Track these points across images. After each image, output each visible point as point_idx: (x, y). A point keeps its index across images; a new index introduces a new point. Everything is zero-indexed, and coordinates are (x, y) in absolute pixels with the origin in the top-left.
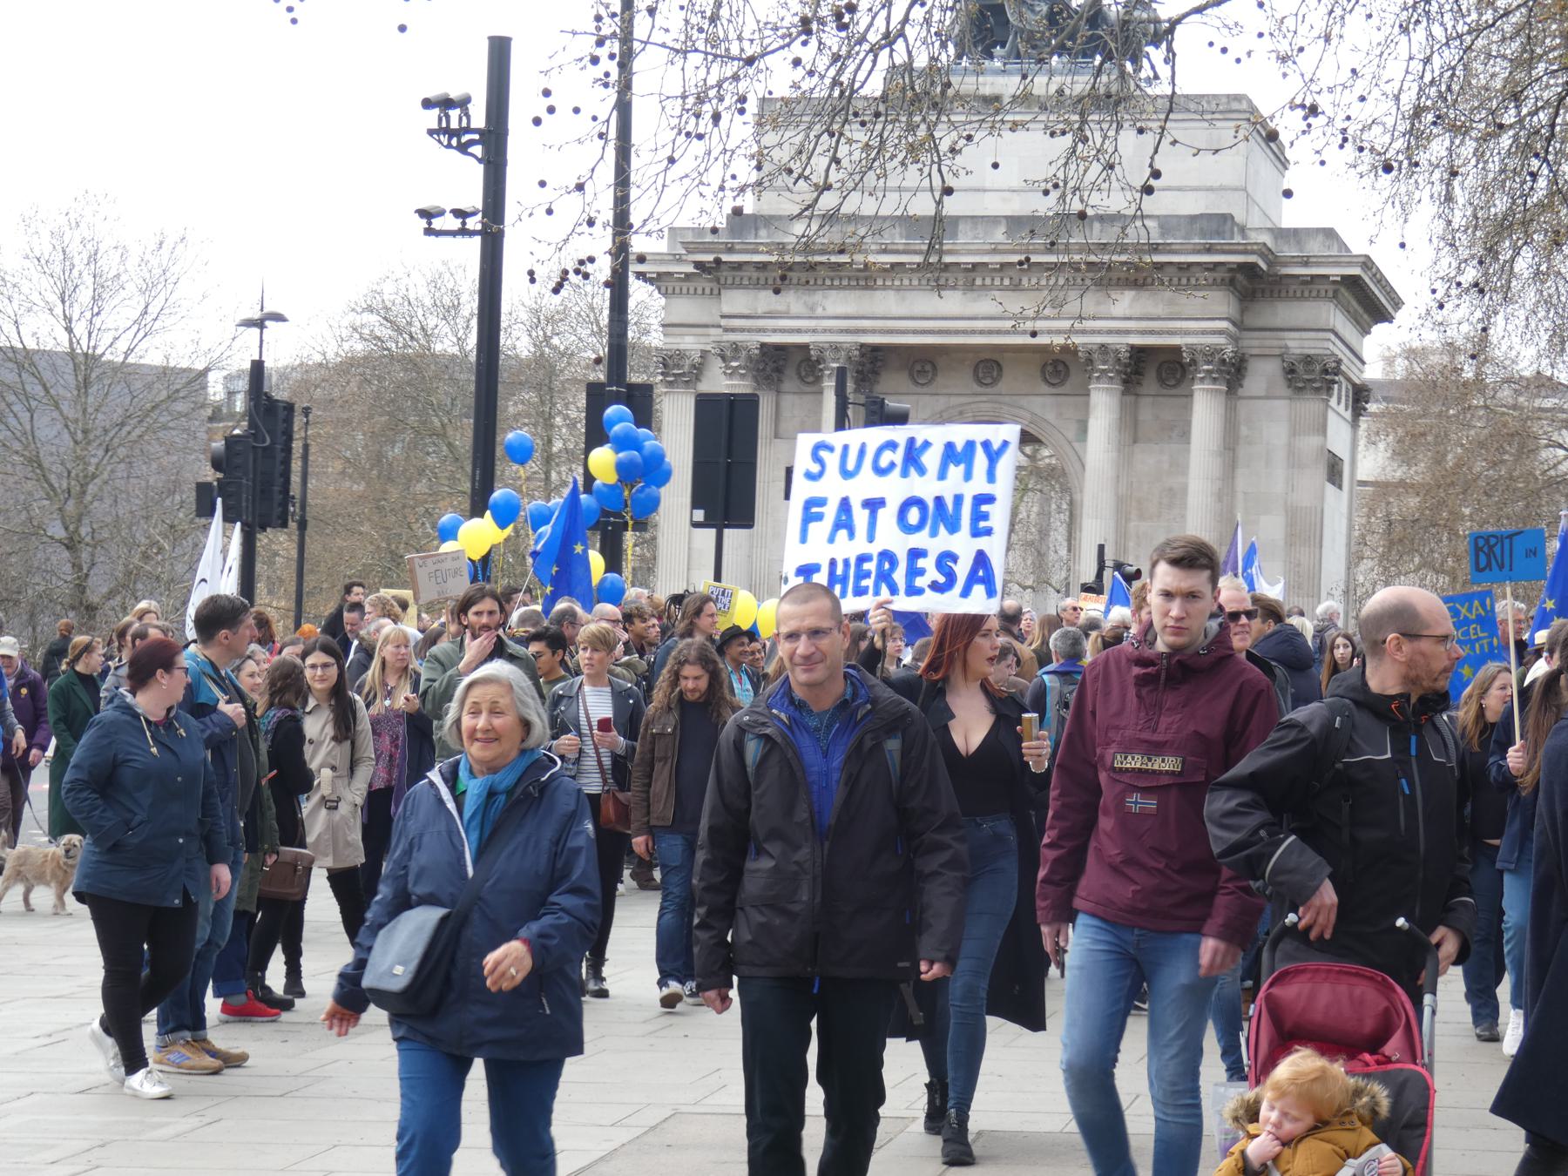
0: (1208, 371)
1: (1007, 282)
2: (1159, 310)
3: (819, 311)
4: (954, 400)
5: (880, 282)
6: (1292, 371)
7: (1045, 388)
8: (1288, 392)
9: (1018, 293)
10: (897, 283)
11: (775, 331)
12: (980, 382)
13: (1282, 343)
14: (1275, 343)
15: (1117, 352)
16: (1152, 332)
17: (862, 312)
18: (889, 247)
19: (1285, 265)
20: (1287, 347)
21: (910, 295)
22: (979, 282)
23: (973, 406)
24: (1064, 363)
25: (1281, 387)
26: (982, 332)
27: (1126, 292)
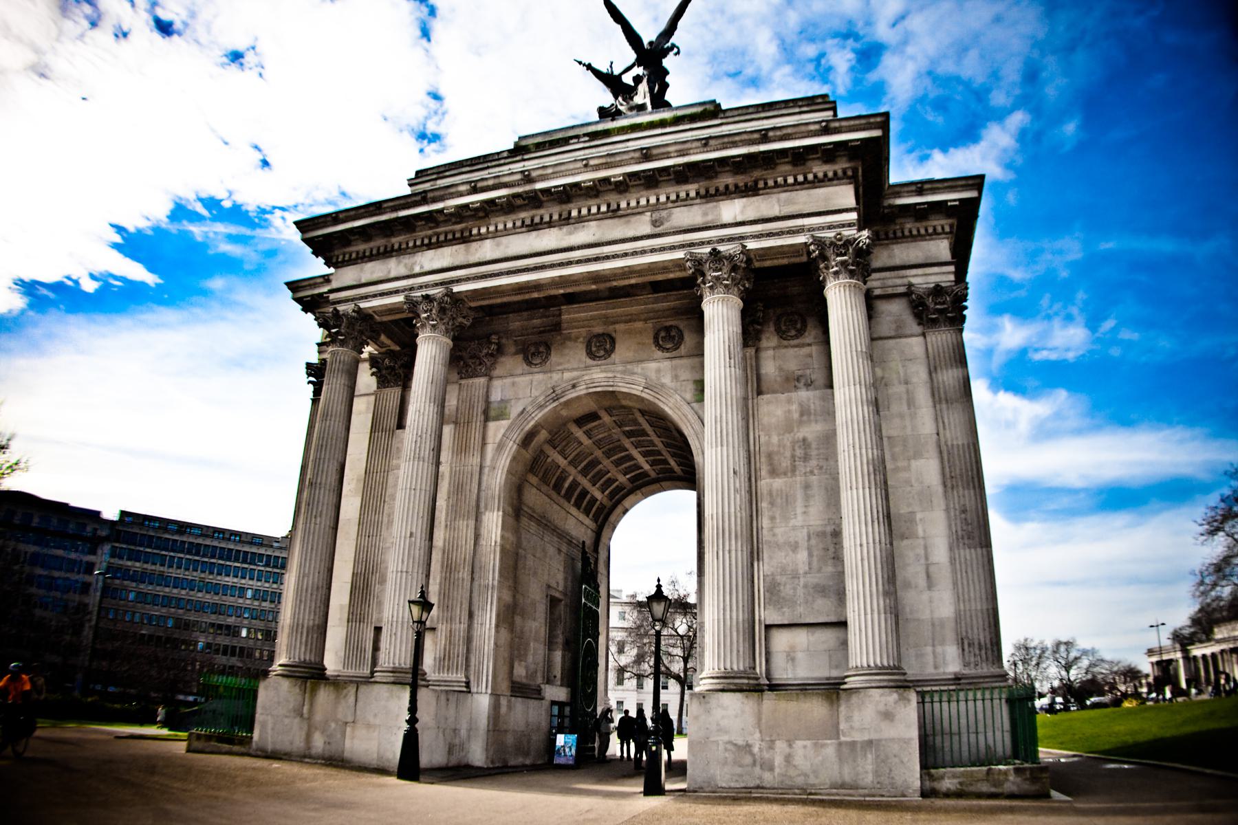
0: (843, 263)
1: (604, 208)
2: (776, 212)
3: (417, 270)
4: (567, 375)
5: (475, 231)
6: (923, 304)
7: (659, 354)
8: (917, 329)
9: (616, 221)
10: (492, 228)
11: (375, 296)
12: (591, 355)
13: (905, 281)
14: (899, 281)
15: (730, 258)
16: (770, 235)
17: (457, 263)
18: (480, 185)
19: (898, 195)
20: (910, 285)
21: (504, 240)
22: (574, 213)
23: (586, 378)
24: (677, 328)
25: (913, 326)
26: (579, 262)
27: (736, 200)
